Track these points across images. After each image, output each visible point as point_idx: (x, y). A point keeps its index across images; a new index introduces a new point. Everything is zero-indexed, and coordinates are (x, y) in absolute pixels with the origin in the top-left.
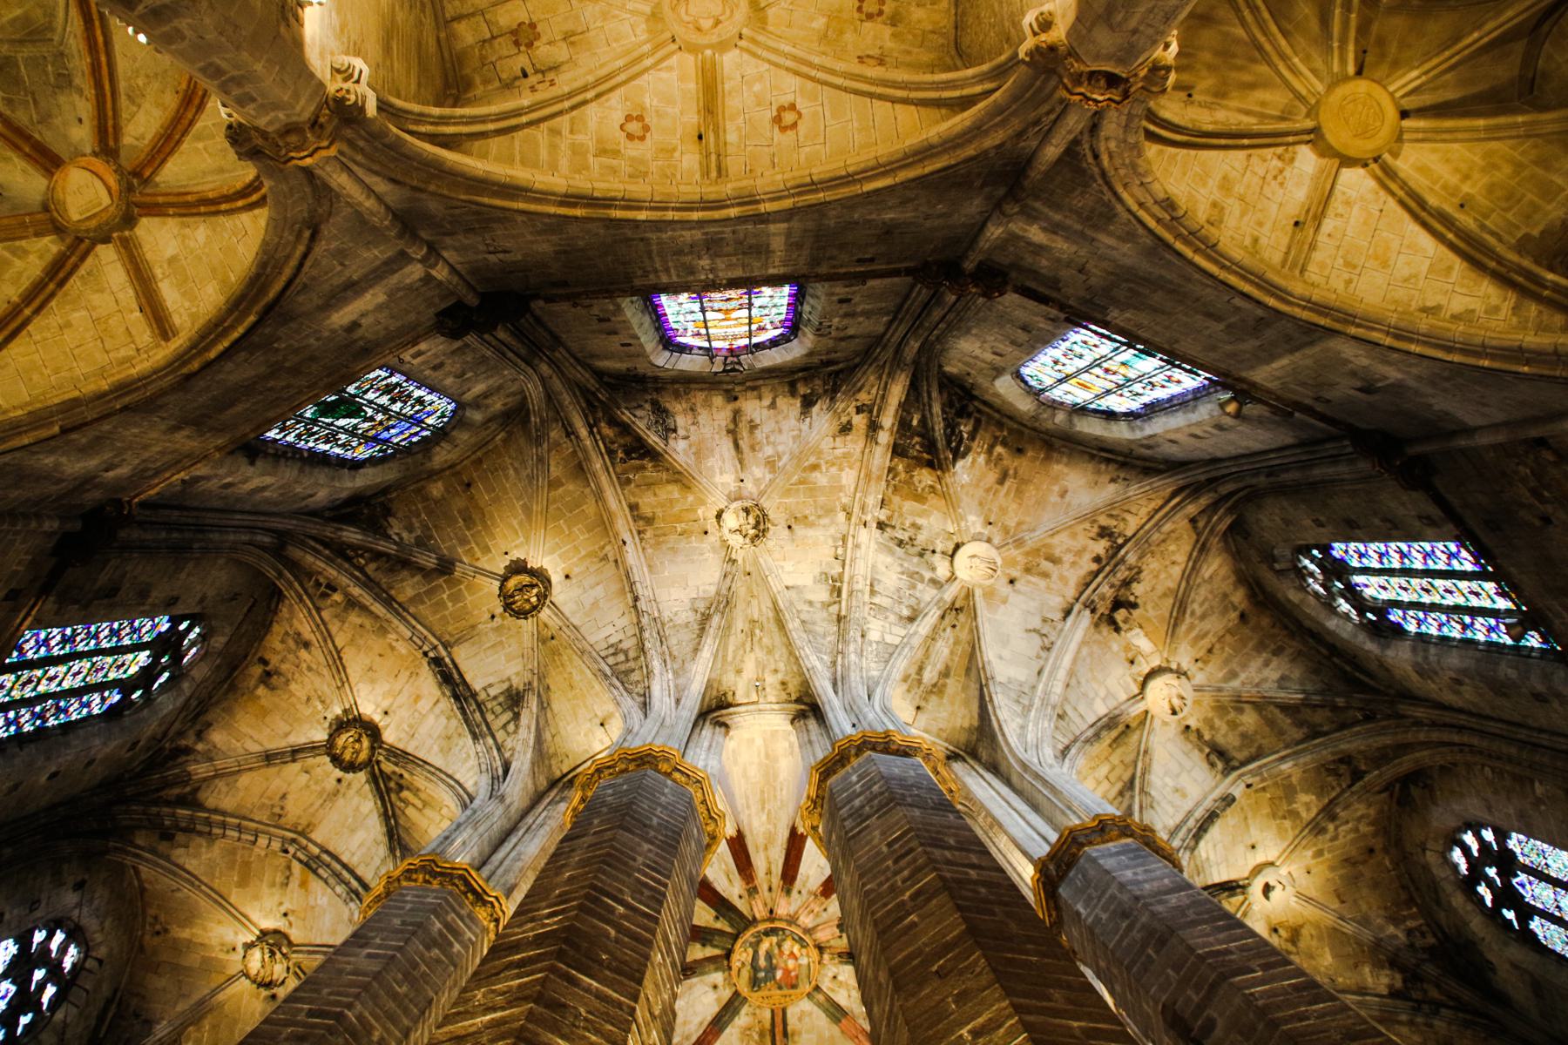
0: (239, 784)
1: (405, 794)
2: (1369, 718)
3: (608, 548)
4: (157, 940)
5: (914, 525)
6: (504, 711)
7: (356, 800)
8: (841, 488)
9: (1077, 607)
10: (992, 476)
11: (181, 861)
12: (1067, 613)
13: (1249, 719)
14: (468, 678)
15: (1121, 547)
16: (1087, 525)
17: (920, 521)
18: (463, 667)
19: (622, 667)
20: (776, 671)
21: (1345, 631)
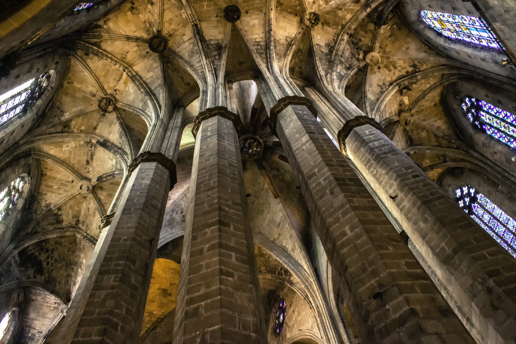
0: (115, 44)
1: (169, 65)
2: (457, 148)
3: (264, 8)
4: (68, 85)
5: (360, 40)
6: (215, 51)
7: (152, 61)
8: (345, 19)
9: (395, 84)
10: (389, 34)
11: (89, 63)
12: (391, 84)
13: (424, 134)
14: (204, 34)
15: (417, 72)
16: (410, 62)
17: (362, 39)
18: (204, 30)
19: (260, 51)
20: (300, 68)
21: (465, 123)
